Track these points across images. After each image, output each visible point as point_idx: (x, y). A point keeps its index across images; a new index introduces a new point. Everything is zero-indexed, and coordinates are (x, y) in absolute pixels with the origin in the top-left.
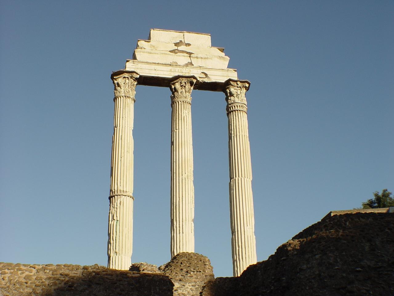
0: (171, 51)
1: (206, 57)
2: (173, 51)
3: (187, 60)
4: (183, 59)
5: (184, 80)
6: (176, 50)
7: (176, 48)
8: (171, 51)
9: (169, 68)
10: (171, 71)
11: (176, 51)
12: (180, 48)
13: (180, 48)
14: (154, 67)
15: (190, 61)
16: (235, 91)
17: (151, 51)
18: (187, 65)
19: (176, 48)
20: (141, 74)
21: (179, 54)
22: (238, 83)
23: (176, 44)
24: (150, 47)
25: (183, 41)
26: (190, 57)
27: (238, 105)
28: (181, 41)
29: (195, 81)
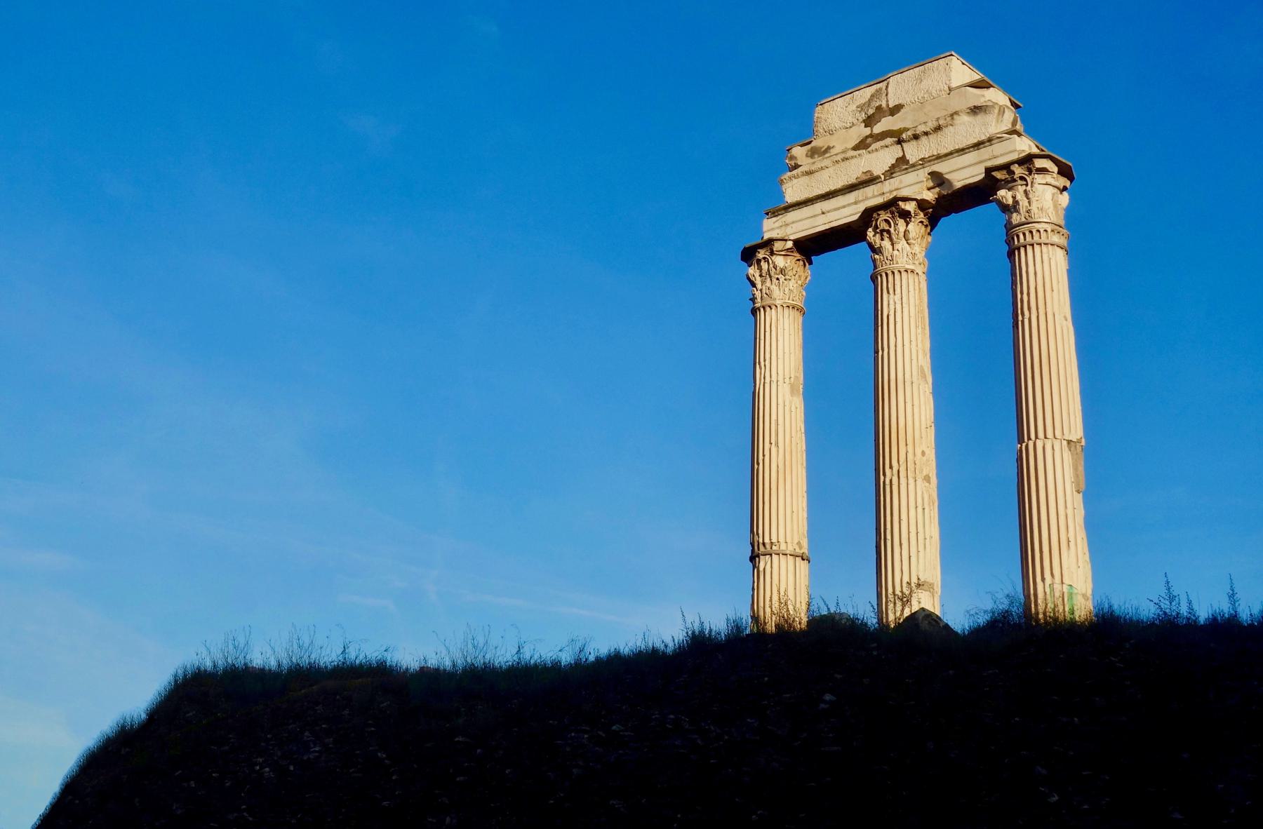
0: (856, 148)
1: (935, 124)
2: (862, 145)
3: (896, 152)
4: (880, 159)
5: (884, 215)
6: (867, 137)
7: (867, 131)
8: (856, 148)
9: (852, 197)
10: (856, 203)
11: (869, 140)
12: (878, 129)
13: (878, 129)
14: (819, 207)
15: (901, 155)
16: (1010, 193)
17: (813, 168)
18: (890, 173)
19: (867, 131)
20: (792, 238)
21: (873, 147)
22: (1016, 168)
23: (869, 121)
24: (812, 157)
25: (884, 105)
26: (900, 142)
27: (1041, 227)
28: (879, 108)
29: (910, 207)
